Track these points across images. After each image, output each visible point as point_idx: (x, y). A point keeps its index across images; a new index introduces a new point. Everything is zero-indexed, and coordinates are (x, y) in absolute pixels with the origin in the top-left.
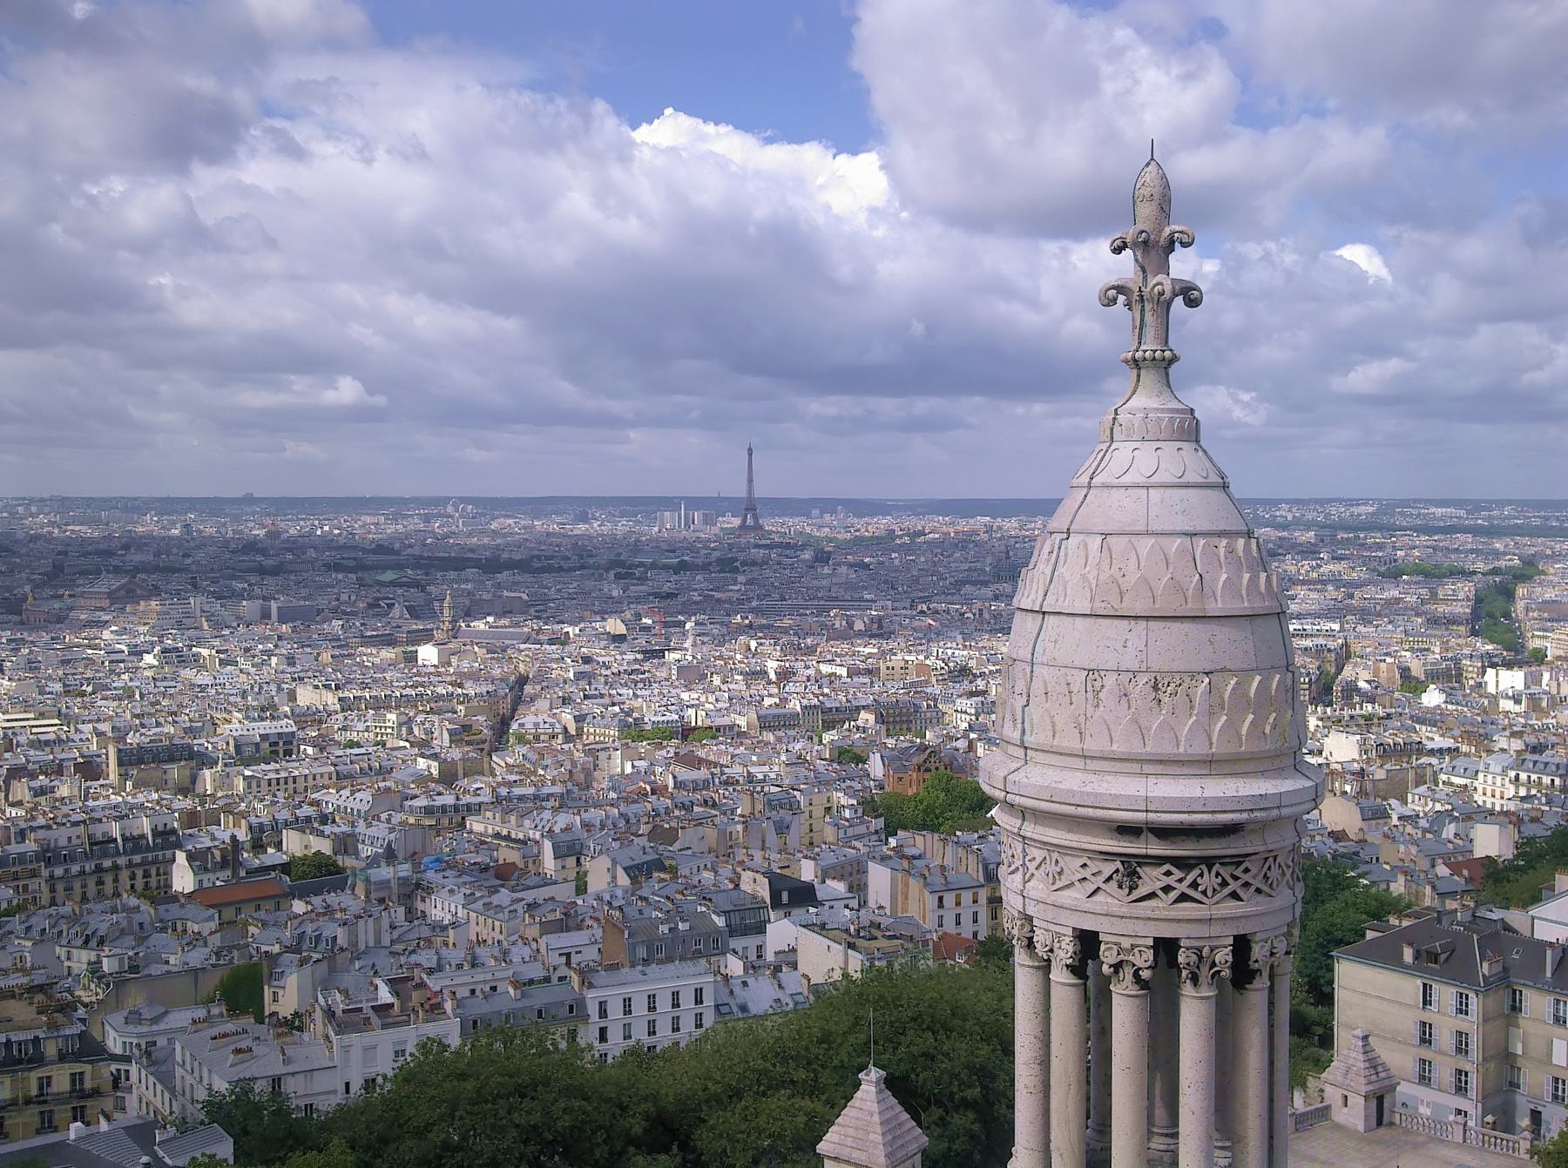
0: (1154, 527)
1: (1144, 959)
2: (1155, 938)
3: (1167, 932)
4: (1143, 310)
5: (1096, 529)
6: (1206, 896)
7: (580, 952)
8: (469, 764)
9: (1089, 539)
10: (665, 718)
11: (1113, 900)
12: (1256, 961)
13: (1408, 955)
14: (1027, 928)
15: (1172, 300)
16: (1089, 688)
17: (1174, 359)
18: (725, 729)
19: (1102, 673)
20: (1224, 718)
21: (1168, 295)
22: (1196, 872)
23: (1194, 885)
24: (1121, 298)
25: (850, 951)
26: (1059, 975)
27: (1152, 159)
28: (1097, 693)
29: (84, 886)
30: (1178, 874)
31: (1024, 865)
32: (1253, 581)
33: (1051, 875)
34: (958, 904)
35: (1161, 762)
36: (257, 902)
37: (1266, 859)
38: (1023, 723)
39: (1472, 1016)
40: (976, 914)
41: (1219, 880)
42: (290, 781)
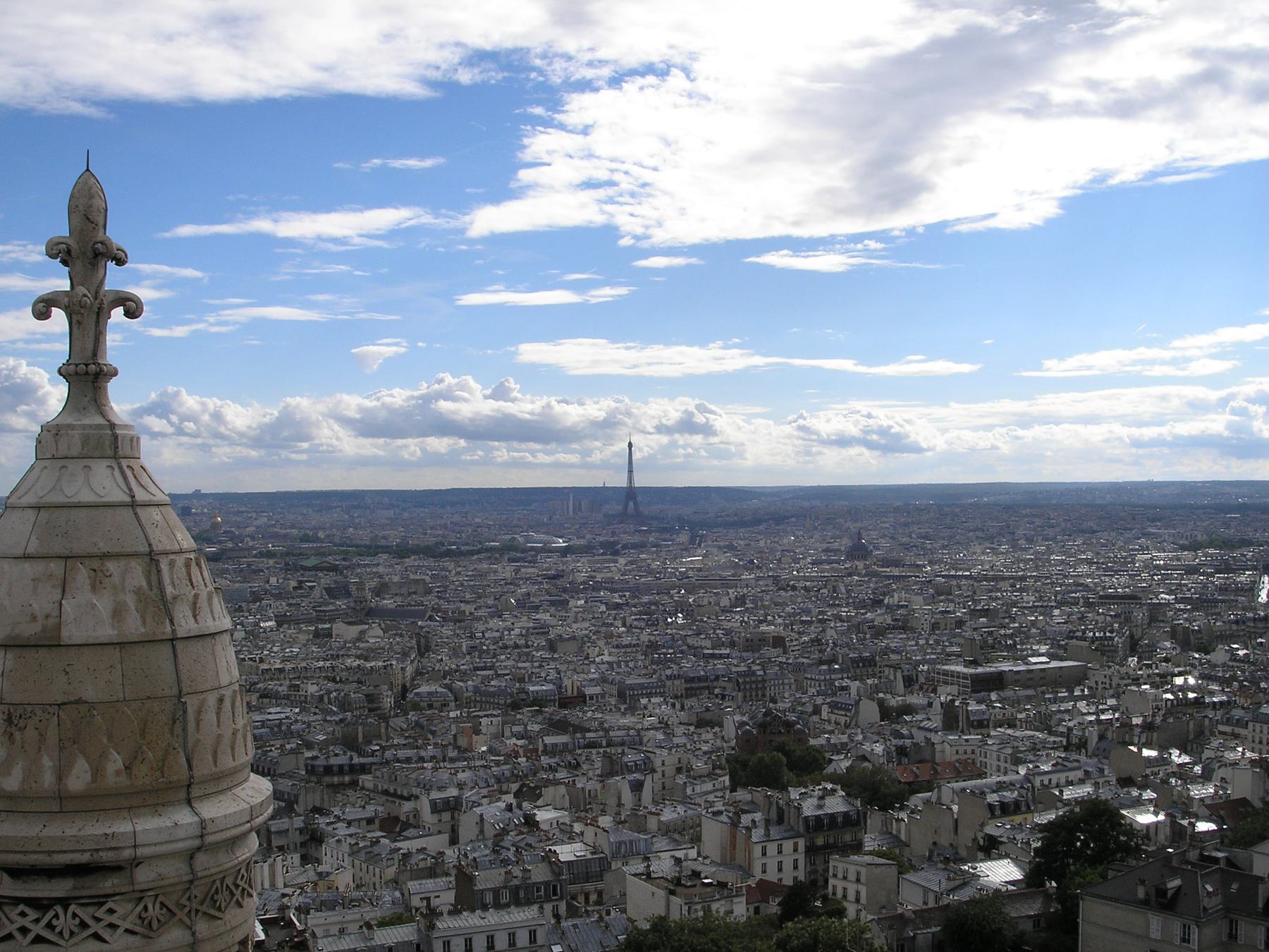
6: (63, 938)
7: (438, 897)
8: (367, 728)
10: (544, 688)
17: (115, 373)
18: (597, 697)
22: (51, 913)
25: (673, 898)
27: (88, 170)
30: (33, 915)
34: (780, 852)
37: (141, 899)
39: (1194, 944)
40: (796, 861)
41: (77, 921)
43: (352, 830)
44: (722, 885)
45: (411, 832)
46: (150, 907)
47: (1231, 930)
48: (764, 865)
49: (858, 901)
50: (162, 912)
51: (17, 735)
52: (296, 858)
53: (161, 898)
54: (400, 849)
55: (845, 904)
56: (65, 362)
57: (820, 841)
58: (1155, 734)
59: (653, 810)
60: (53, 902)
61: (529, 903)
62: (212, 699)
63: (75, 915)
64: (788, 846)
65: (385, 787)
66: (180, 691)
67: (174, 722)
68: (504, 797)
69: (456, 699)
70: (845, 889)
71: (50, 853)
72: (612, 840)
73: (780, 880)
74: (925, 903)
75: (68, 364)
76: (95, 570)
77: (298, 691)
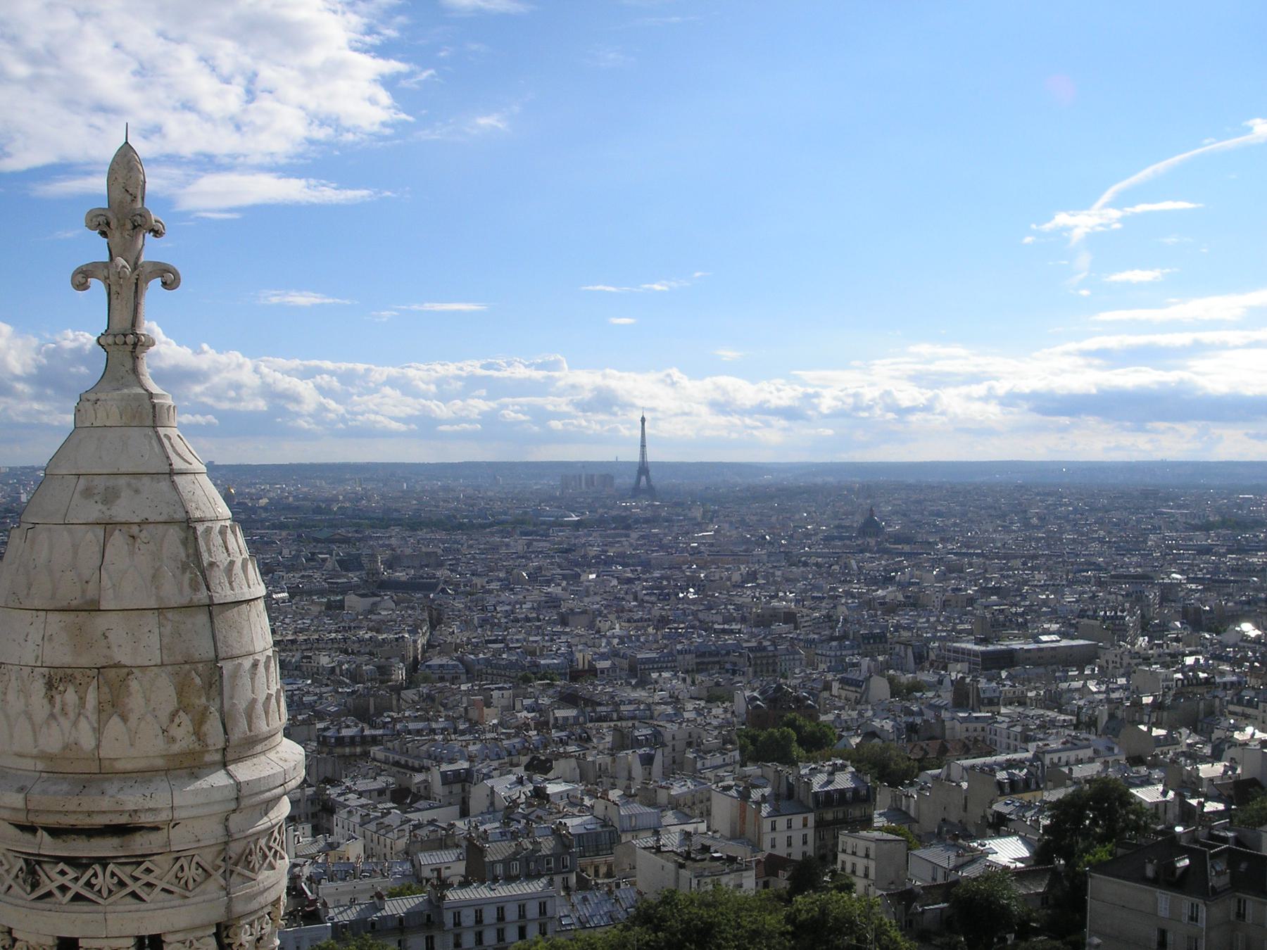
2: (59, 938)
6: (102, 897)
7: (449, 868)
10: (555, 661)
18: (608, 671)
19: (10, 667)
22: (90, 872)
23: (89, 884)
25: (682, 871)
27: (127, 142)
30: (72, 874)
34: (789, 827)
37: (177, 859)
40: (805, 836)
43: (363, 801)
44: (731, 859)
45: (422, 804)
46: (186, 868)
47: (1239, 909)
48: (773, 840)
49: (866, 876)
50: (197, 872)
51: (58, 698)
52: (308, 828)
53: (196, 859)
54: (410, 820)
55: (854, 879)
56: (103, 332)
57: (829, 816)
58: (1165, 714)
59: (664, 784)
60: (92, 861)
61: (538, 876)
62: (247, 663)
63: (113, 874)
64: (797, 820)
65: (397, 758)
66: (217, 656)
67: (211, 687)
68: (514, 769)
69: (467, 672)
70: (854, 865)
71: (90, 814)
72: (622, 813)
73: (789, 855)
74: (934, 879)
75: (106, 334)
76: (133, 537)
77: (310, 662)
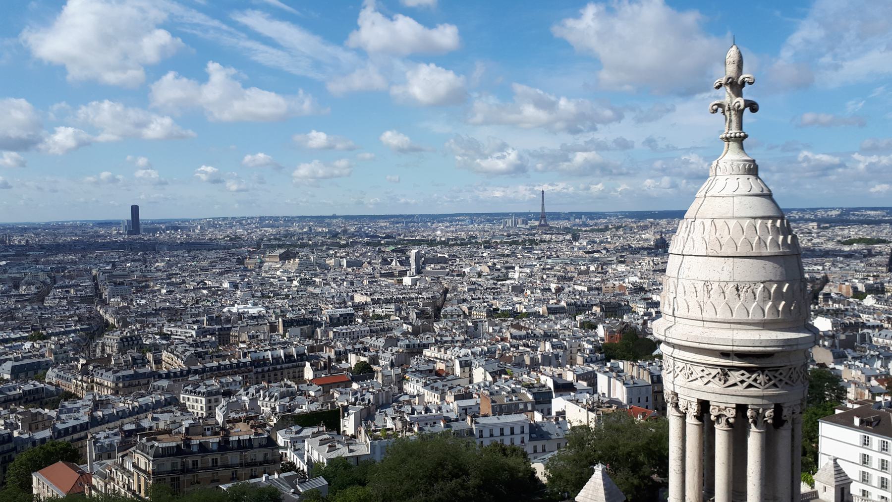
0: (736, 215)
1: (731, 414)
2: (737, 404)
3: (742, 401)
4: (730, 114)
5: (708, 217)
9: (705, 221)
10: (507, 309)
11: (717, 386)
12: (785, 416)
13: (857, 421)
14: (675, 398)
15: (743, 110)
16: (706, 289)
17: (746, 136)
20: (770, 303)
21: (742, 107)
23: (755, 380)
24: (720, 110)
25: (589, 412)
26: (691, 420)
28: (709, 292)
29: (269, 376)
30: (747, 375)
31: (674, 370)
32: (785, 239)
33: (687, 375)
35: (740, 323)
36: (337, 385)
37: (790, 369)
38: (674, 305)
41: (767, 378)
42: (352, 333)
